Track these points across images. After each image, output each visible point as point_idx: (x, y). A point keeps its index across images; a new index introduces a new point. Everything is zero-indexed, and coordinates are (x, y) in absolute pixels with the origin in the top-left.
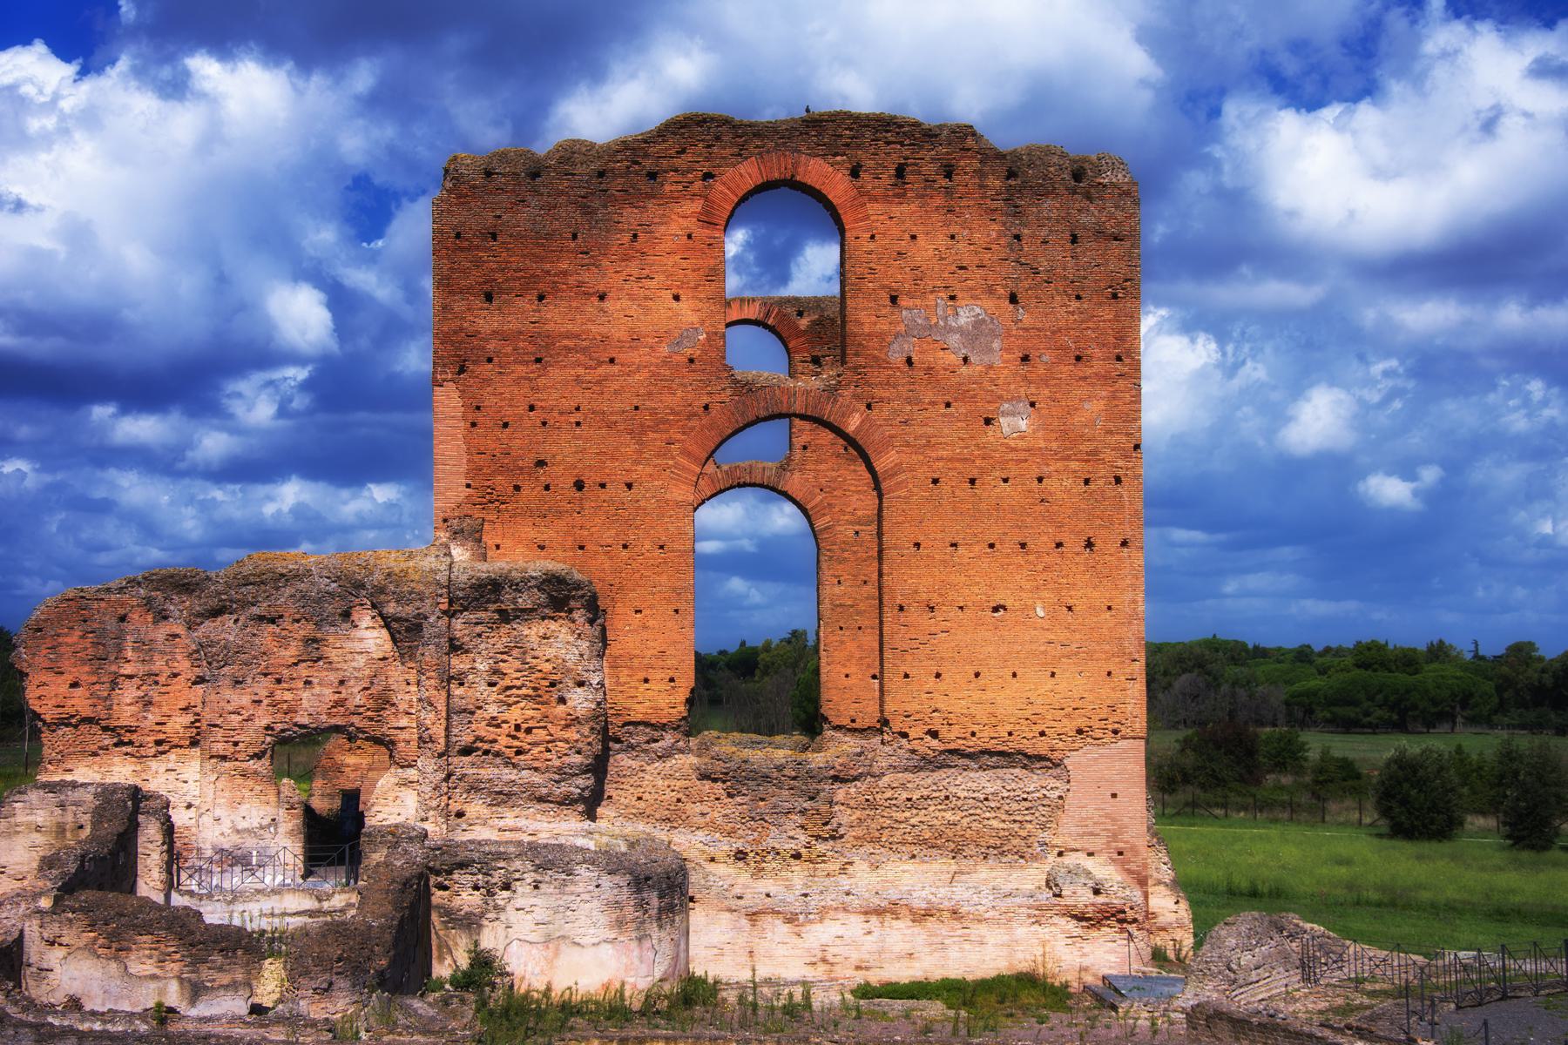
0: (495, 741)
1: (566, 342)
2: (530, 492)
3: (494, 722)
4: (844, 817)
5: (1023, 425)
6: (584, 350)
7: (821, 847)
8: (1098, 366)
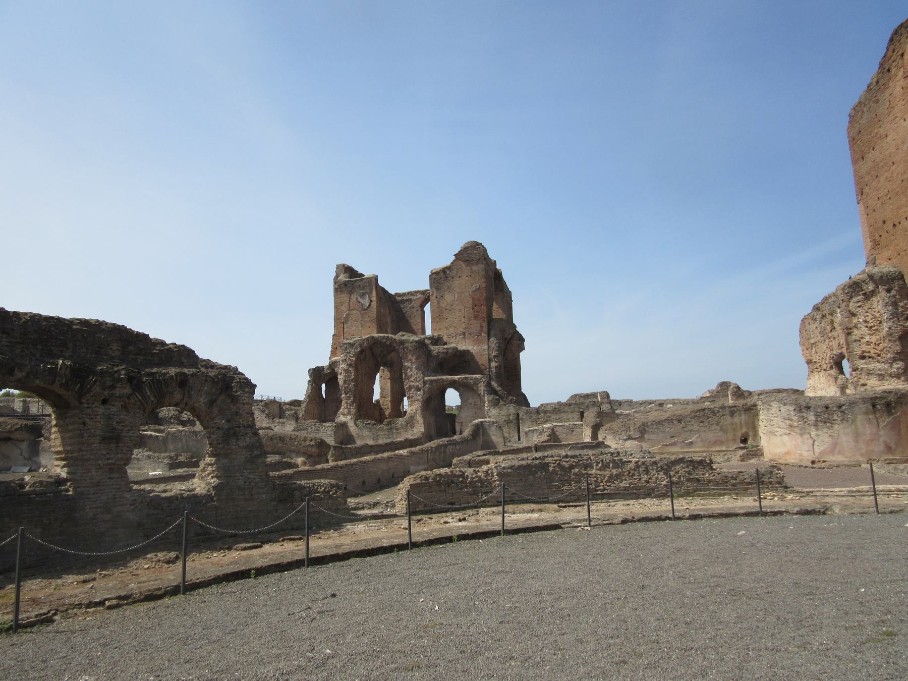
0: (869, 352)
1: (881, 164)
2: (884, 235)
3: (868, 343)
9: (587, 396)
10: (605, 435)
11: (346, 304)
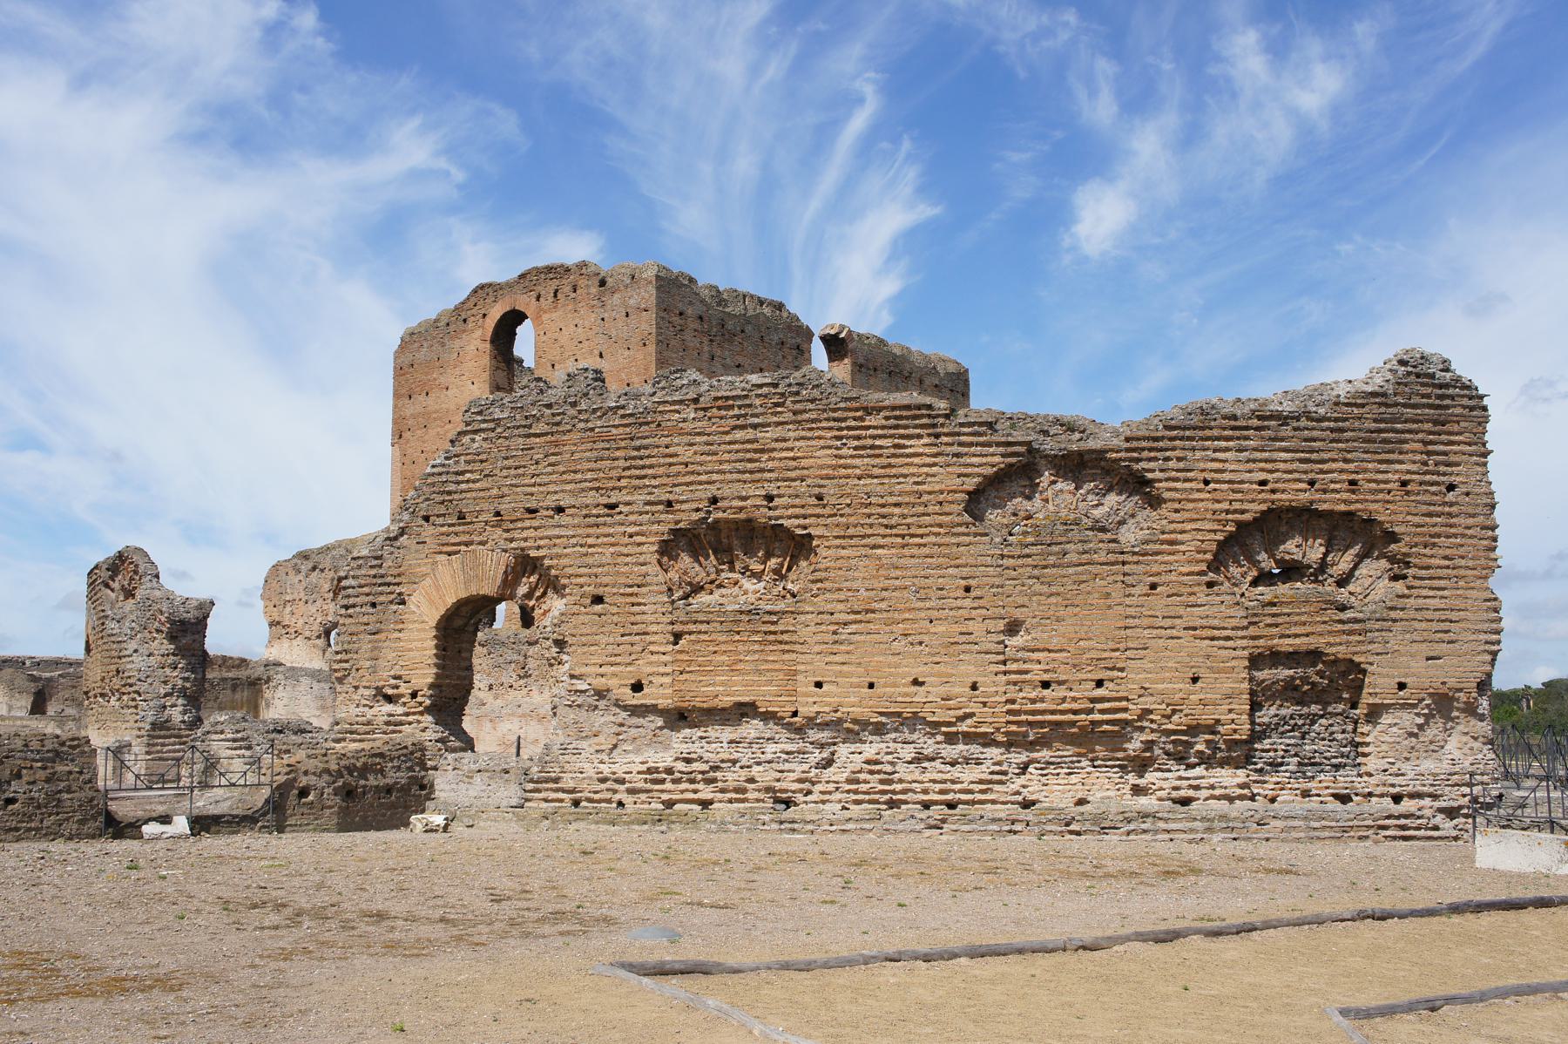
1: (435, 415)
4: (532, 664)
6: (440, 419)
7: (522, 682)
10: (62, 707)
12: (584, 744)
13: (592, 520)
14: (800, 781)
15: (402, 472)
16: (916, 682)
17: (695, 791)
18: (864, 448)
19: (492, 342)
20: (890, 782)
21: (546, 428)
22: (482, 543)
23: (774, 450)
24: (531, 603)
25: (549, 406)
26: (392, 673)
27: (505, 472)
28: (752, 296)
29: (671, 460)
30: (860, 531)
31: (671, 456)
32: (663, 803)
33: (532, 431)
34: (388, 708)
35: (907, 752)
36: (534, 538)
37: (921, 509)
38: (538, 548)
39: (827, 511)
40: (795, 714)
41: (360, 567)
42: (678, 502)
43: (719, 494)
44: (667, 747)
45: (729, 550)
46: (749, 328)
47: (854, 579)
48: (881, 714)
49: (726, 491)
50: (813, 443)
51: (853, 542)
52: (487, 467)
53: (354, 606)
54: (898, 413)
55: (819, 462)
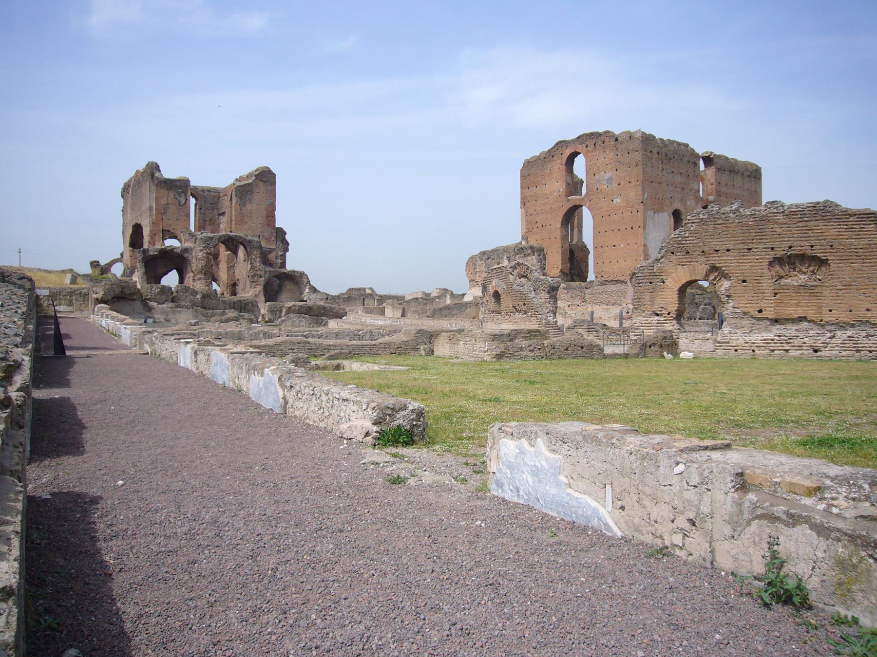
2: (535, 228)
4: (587, 296)
5: (618, 200)
7: (583, 304)
8: (633, 184)
9: (359, 289)
11: (165, 199)
12: (738, 331)
13: (741, 254)
14: (823, 343)
15: (526, 218)
16: (868, 310)
17: (783, 346)
18: (849, 228)
19: (566, 165)
20: (857, 344)
21: (723, 222)
22: (696, 262)
23: (814, 229)
24: (715, 282)
25: (724, 214)
26: (660, 306)
27: (706, 237)
28: (677, 142)
29: (773, 233)
30: (848, 258)
31: (773, 232)
32: (770, 350)
33: (717, 223)
34: (657, 318)
35: (864, 334)
36: (715, 260)
37: (871, 250)
38: (720, 263)
39: (834, 251)
40: (821, 321)
41: (644, 269)
42: (776, 248)
43: (792, 245)
44: (771, 332)
45: (794, 264)
46: (676, 156)
47: (845, 274)
48: (854, 321)
49: (795, 244)
50: (829, 227)
51: (844, 261)
52: (699, 236)
53: (642, 283)
54: (862, 216)
55: (832, 233)
